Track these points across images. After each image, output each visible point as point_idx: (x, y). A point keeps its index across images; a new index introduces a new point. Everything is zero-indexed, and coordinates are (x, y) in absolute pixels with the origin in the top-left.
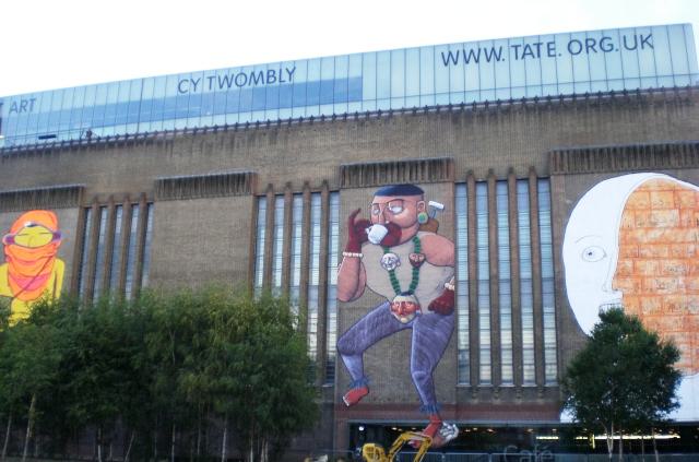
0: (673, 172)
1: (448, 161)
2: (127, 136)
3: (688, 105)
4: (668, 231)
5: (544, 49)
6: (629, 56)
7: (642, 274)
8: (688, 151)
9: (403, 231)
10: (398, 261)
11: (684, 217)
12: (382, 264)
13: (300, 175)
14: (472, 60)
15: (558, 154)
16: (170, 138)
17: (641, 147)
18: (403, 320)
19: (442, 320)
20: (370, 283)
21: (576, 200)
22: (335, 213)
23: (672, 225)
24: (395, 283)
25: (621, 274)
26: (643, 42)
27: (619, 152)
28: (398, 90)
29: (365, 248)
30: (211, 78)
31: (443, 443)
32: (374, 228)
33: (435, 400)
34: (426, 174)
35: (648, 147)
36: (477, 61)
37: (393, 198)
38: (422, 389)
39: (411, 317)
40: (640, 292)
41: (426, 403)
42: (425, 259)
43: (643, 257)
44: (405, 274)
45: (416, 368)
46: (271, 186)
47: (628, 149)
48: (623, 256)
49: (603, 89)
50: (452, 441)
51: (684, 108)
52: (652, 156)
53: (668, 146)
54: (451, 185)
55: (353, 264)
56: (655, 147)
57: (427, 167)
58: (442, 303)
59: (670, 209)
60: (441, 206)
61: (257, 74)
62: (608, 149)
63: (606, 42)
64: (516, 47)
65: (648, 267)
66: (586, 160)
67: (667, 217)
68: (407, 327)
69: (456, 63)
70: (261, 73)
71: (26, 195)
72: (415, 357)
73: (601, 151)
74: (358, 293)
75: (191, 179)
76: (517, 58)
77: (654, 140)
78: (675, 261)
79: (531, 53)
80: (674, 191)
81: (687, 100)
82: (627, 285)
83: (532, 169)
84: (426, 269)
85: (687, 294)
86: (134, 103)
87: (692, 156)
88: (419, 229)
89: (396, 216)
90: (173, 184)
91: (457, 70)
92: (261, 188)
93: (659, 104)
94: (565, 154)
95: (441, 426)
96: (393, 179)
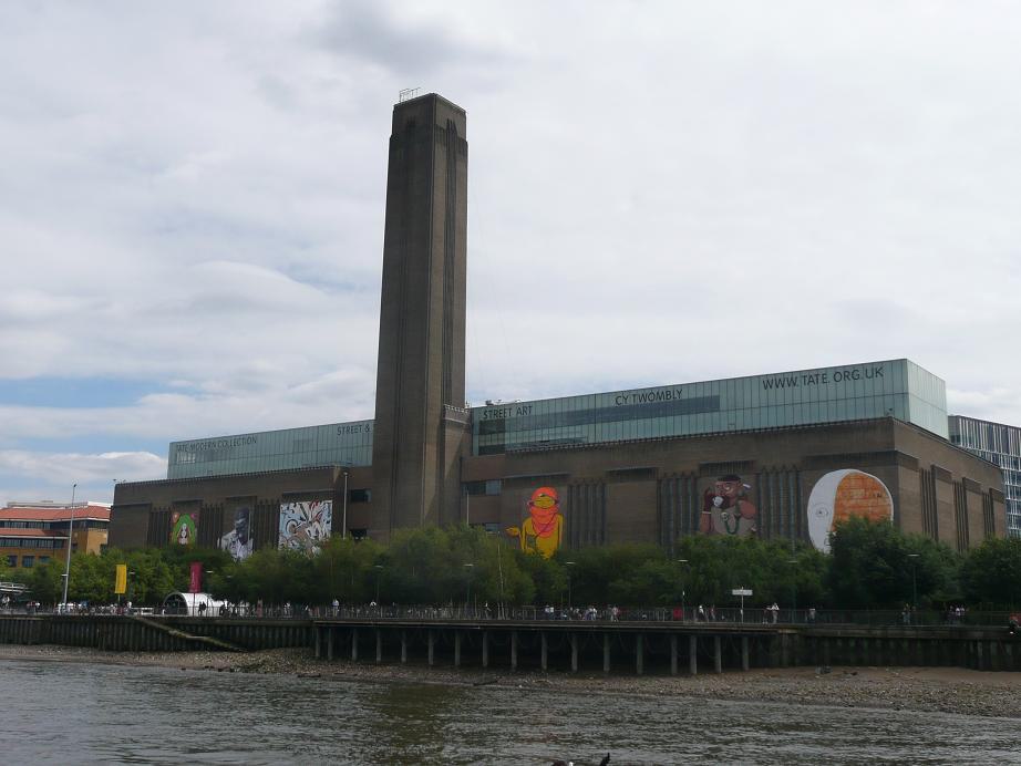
5: (820, 378)
21: (814, 484)
44: (732, 523)
48: (836, 514)
63: (856, 373)
71: (538, 478)
80: (863, 478)
84: (742, 520)
91: (772, 391)
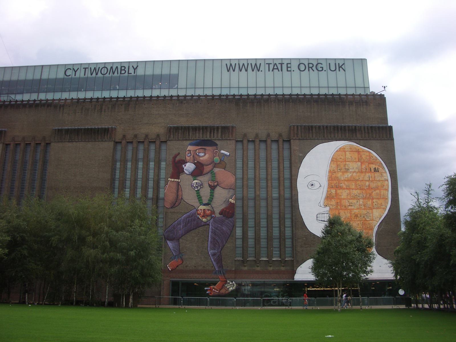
0: (357, 141)
1: (233, 127)
2: (23, 101)
3: (367, 105)
4: (354, 174)
6: (332, 74)
7: (340, 197)
8: (366, 129)
9: (205, 167)
10: (202, 184)
11: (364, 166)
12: (192, 186)
13: (143, 130)
14: (243, 69)
15: (296, 127)
16: (62, 104)
17: (341, 126)
18: (204, 220)
19: (227, 221)
20: (185, 197)
22: (163, 155)
23: (357, 171)
24: (199, 198)
25: (329, 197)
26: (339, 67)
27: (329, 128)
28: (200, 84)
29: (182, 176)
30: (85, 69)
31: (227, 292)
32: (188, 164)
33: (222, 267)
34: (220, 134)
35: (345, 127)
36: (246, 70)
37: (200, 147)
38: (215, 261)
39: (209, 218)
40: (339, 207)
41: (217, 269)
42: (218, 185)
43: (341, 188)
44: (206, 192)
45: (211, 249)
46: (124, 136)
47: (334, 127)
48: (330, 187)
49: (335, 92)
50: (232, 291)
51: (365, 106)
52: (347, 131)
53: (355, 127)
54: (234, 141)
55: (174, 186)
56: (349, 126)
57: (220, 131)
58: (228, 210)
59: (356, 162)
60: (228, 154)
61: (114, 68)
62: (323, 126)
63: (320, 65)
64: (269, 64)
65: (344, 194)
66: (311, 131)
67: (354, 166)
68: (206, 224)
69: (234, 71)
70: (117, 67)
72: (211, 242)
73: (319, 127)
74: (177, 203)
75: (75, 130)
76: (269, 71)
77: (348, 123)
78: (359, 191)
79: (278, 69)
80: (358, 152)
81: (366, 102)
82: (332, 203)
83: (280, 135)
84: (218, 190)
85: (364, 209)
86: (36, 80)
87: (368, 133)
88: (214, 167)
89: (201, 158)
90: (64, 133)
91: (234, 75)
92: (118, 138)
93: (351, 103)
94: (299, 128)
95: (226, 282)
96: (199, 136)
